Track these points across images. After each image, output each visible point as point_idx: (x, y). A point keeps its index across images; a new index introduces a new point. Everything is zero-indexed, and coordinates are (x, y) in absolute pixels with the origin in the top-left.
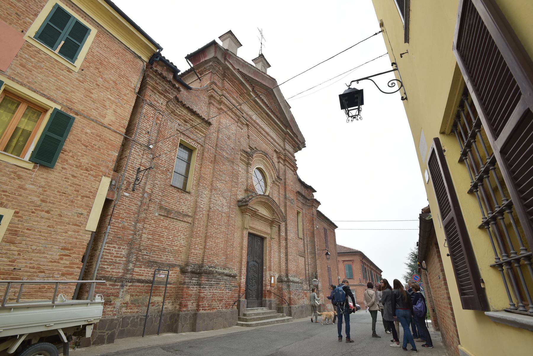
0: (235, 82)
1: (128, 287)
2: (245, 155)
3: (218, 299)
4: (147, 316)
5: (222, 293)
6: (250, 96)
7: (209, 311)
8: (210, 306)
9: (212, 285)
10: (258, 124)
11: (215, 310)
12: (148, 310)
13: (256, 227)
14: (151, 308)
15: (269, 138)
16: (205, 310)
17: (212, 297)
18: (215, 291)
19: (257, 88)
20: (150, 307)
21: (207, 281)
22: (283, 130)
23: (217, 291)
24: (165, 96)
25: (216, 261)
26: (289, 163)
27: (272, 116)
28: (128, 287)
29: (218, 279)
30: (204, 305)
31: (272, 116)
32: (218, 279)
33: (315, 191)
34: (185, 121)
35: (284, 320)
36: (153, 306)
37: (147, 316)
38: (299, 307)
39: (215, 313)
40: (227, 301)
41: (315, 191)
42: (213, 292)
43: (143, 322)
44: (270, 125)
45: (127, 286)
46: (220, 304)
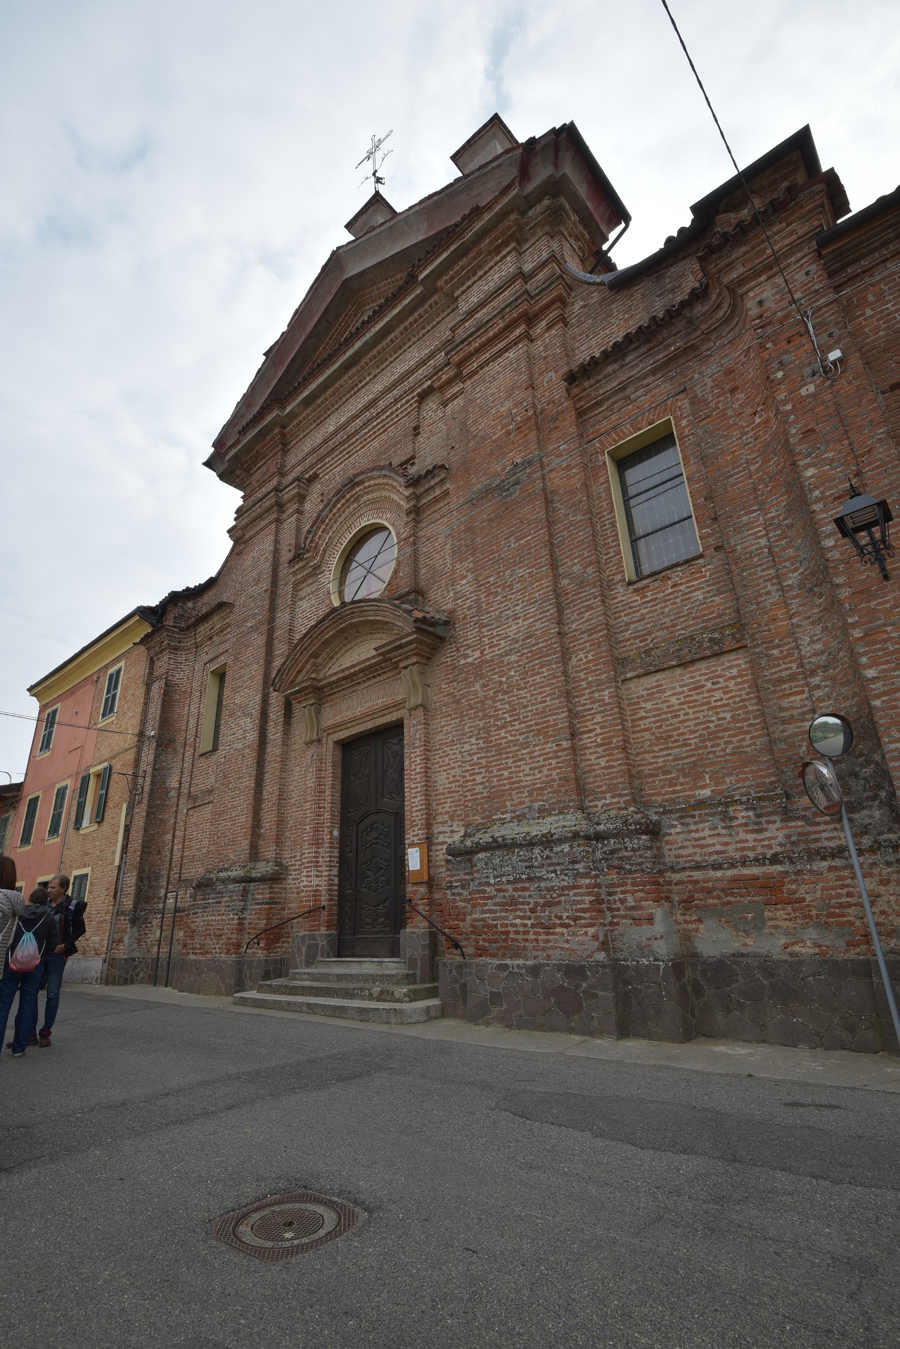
0: (258, 452)
2: (301, 564)
4: (158, 958)
6: (292, 415)
7: (201, 958)
8: (203, 946)
9: (205, 907)
13: (349, 715)
15: (382, 404)
16: (196, 954)
17: (206, 930)
21: (203, 899)
22: (420, 301)
23: (213, 918)
25: (232, 856)
26: (478, 351)
27: (358, 345)
29: (219, 893)
31: (358, 345)
35: (343, 1009)
38: (535, 971)
39: (206, 961)
40: (229, 939)
42: (208, 921)
44: (381, 362)
46: (218, 943)
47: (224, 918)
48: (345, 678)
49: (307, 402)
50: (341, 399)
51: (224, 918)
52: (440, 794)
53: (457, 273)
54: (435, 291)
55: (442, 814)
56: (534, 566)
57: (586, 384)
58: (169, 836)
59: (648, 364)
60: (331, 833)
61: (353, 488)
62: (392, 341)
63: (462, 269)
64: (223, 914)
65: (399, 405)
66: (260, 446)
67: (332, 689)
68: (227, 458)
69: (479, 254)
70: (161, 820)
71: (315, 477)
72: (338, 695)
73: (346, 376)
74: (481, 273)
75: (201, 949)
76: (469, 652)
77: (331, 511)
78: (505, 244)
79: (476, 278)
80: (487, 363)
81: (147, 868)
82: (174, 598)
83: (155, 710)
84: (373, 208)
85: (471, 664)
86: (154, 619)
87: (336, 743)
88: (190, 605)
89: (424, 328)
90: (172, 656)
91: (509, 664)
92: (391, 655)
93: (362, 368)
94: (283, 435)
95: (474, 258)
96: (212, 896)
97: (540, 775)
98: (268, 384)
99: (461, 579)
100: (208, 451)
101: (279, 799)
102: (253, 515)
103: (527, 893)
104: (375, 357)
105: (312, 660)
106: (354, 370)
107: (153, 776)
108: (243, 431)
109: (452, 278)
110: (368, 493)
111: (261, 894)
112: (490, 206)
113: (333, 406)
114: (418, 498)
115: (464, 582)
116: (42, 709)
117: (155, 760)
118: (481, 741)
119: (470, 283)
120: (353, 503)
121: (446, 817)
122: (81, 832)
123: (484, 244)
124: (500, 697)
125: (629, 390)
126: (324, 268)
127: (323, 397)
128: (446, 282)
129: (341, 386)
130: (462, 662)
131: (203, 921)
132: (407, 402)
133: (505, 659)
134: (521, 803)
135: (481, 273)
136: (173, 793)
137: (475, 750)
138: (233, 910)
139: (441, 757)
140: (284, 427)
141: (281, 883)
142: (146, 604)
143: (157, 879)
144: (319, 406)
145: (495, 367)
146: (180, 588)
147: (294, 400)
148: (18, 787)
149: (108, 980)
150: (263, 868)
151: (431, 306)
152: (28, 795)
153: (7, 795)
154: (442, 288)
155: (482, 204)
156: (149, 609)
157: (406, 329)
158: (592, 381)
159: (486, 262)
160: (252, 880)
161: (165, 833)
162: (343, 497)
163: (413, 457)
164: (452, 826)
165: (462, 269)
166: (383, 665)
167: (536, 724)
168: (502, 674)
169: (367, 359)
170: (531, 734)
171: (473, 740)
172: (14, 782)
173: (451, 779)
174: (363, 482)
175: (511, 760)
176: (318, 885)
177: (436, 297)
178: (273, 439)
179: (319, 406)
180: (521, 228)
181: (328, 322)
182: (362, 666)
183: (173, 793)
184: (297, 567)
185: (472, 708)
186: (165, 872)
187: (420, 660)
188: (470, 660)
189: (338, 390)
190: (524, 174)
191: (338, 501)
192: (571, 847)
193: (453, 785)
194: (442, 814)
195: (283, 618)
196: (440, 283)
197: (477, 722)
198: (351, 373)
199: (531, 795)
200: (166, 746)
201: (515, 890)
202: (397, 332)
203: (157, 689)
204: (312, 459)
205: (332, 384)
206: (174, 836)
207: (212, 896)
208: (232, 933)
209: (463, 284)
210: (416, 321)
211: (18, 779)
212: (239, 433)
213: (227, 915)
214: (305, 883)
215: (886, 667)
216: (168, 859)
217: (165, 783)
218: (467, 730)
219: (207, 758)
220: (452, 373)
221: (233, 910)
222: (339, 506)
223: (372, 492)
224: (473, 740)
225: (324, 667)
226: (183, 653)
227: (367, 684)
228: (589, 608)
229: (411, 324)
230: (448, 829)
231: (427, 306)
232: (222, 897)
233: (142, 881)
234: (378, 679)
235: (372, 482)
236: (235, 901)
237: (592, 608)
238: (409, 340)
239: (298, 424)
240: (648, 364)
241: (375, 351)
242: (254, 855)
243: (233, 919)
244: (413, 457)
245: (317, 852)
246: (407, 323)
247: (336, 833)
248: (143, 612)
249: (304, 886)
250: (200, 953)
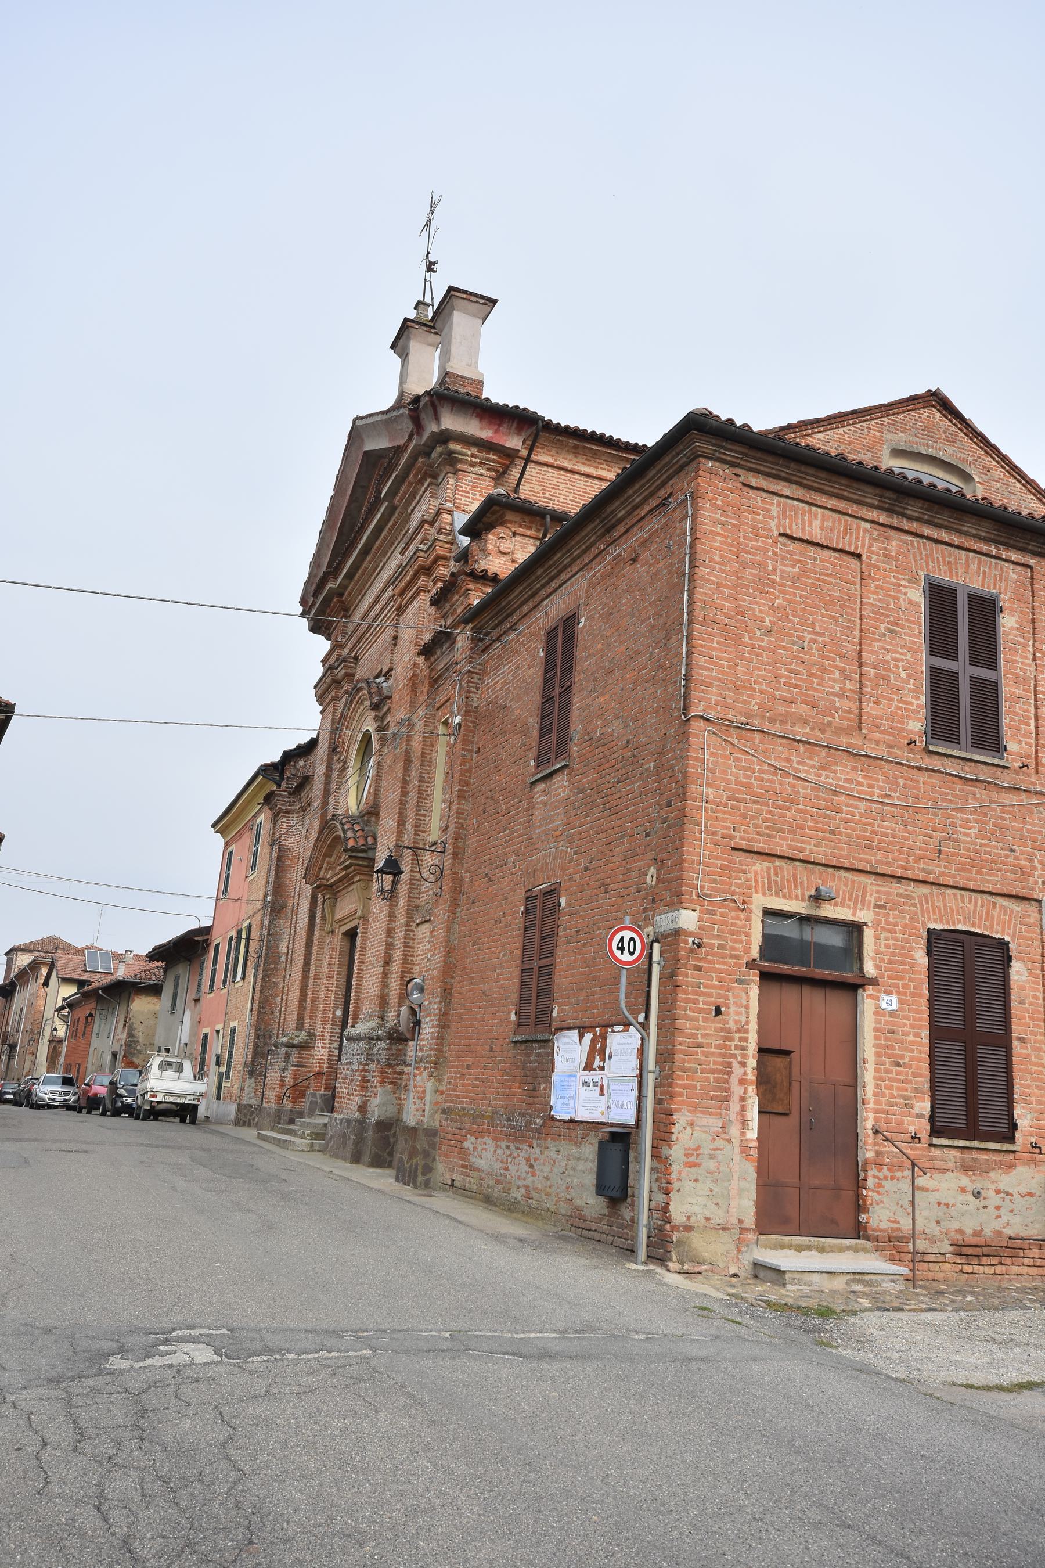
6: (343, 587)
15: (382, 602)
58: (279, 999)
60: (334, 1013)
69: (410, 484)
79: (415, 501)
81: (262, 1026)
82: (289, 756)
88: (301, 763)
90: (285, 820)
94: (343, 602)
98: (328, 546)
107: (268, 941)
108: (315, 595)
114: (382, 719)
116: (227, 844)
122: (237, 986)
126: (350, 435)
136: (283, 959)
140: (341, 595)
142: (268, 761)
148: (207, 930)
149: (237, 1123)
150: (303, 1035)
152: (216, 938)
153: (199, 938)
156: (274, 766)
159: (419, 490)
160: (293, 1046)
163: (391, 670)
172: (203, 925)
180: (431, 466)
181: (363, 487)
183: (283, 959)
186: (275, 1032)
187: (362, 877)
190: (418, 426)
191: (352, 701)
200: (279, 912)
211: (207, 922)
217: (278, 947)
242: (300, 1026)
244: (391, 670)
248: (266, 770)
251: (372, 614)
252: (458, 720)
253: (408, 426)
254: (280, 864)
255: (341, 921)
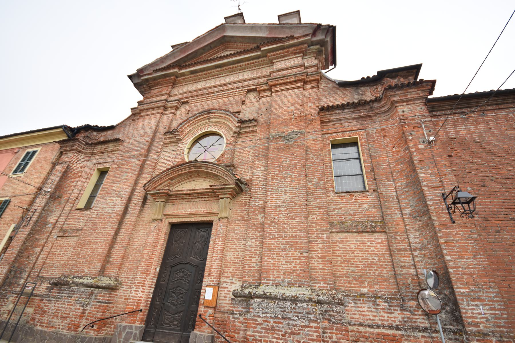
0: (159, 82)
1: (13, 298)
2: (171, 136)
3: (61, 317)
5: (70, 308)
6: (183, 75)
8: (49, 322)
9: (59, 298)
10: (203, 89)
11: (53, 330)
12: (20, 318)
13: (183, 212)
14: (23, 318)
15: (229, 87)
16: (42, 326)
17: (55, 312)
18: (60, 306)
19: (205, 56)
20: (22, 316)
21: (58, 293)
22: (258, 57)
23: (63, 306)
24: (73, 150)
25: (86, 270)
26: (281, 84)
28: (13, 298)
29: (72, 291)
30: (43, 321)
32: (72, 291)
33: (417, 68)
34: (103, 153)
36: (25, 316)
37: (17, 324)
39: (50, 332)
40: (72, 321)
41: (417, 68)
42: (59, 307)
43: (13, 329)
44: (232, 71)
45: (12, 297)
46: (62, 322)
47: (71, 307)
48: (186, 194)
49: (192, 72)
50: (208, 77)
51: (71, 307)
52: (228, 262)
53: (277, 54)
54: (266, 56)
55: (227, 272)
56: (297, 173)
57: (327, 113)
58: (39, 249)
59: (352, 116)
60: (156, 269)
61: (209, 113)
62: (240, 66)
63: (280, 54)
64: (72, 305)
65: (238, 90)
66: (161, 80)
67: (177, 197)
68: (142, 78)
69: (288, 52)
70: (36, 239)
71: (187, 102)
72: (178, 201)
73: (215, 70)
74: (286, 58)
75: (47, 324)
76: (257, 200)
77: (195, 119)
78: (299, 53)
80: (284, 90)
81: (17, 265)
82: (87, 128)
83: (55, 178)
84: (239, 17)
85: (257, 206)
86: (70, 134)
87: (170, 223)
88: (95, 133)
89: (255, 67)
90: (76, 154)
91: (279, 211)
92: (217, 191)
93: (223, 70)
94: (175, 80)
95: (286, 52)
96: (66, 292)
97: (290, 266)
98: (175, 58)
99: (258, 168)
100: (134, 71)
101: (127, 245)
102: (150, 106)
103: (281, 326)
104: (230, 68)
105: (169, 181)
106: (219, 69)
107: (41, 213)
109: (274, 55)
110: (215, 118)
111: (102, 296)
112: (298, 38)
113: (204, 78)
114: (241, 128)
115: (259, 169)
117: (45, 205)
118: (258, 242)
119: (281, 60)
120: (207, 119)
121: (230, 275)
123: (291, 49)
124: (273, 224)
125: (342, 122)
127: (201, 73)
128: (272, 55)
129: (211, 73)
130: (253, 204)
131: (55, 306)
132: (241, 90)
133: (278, 209)
134: (279, 277)
135: (286, 58)
136: (50, 225)
137: (254, 246)
138: (81, 303)
139: (232, 244)
140: (177, 77)
141: (116, 292)
143: (21, 273)
144: (197, 76)
145: (288, 93)
146: (92, 124)
147: (186, 69)
150: (105, 281)
151: (261, 61)
154: (269, 56)
155: (295, 36)
157: (248, 64)
158: (329, 113)
159: (289, 56)
161: (36, 247)
162: (202, 115)
163: (240, 112)
164: (232, 280)
165: (280, 54)
166: (210, 194)
167: (291, 242)
168: (275, 214)
169: (227, 67)
170: (288, 246)
171: (253, 241)
173: (236, 256)
174: (214, 113)
175: (276, 256)
176: (141, 297)
177: (265, 59)
178: (170, 79)
179: (197, 76)
180: (306, 51)
181: (211, 47)
182: (199, 191)
183: (50, 225)
184: (168, 136)
185: (255, 226)
188: (257, 204)
189: (209, 73)
190: (314, 34)
191: (200, 116)
192: (307, 305)
193: (237, 259)
194: (227, 272)
195: (152, 156)
196: (269, 54)
197: (257, 233)
198: (217, 69)
199: (284, 274)
200: (55, 199)
201: (274, 322)
202: (244, 63)
203: (60, 169)
204: (189, 95)
205: (207, 70)
206: (42, 250)
207: (66, 292)
208: (75, 318)
209: (278, 59)
210: (253, 63)
212: (154, 71)
213: (75, 305)
214: (133, 295)
215: (454, 257)
216: (33, 262)
217: (47, 218)
218: (250, 235)
219: (81, 211)
220: (266, 88)
221: (81, 303)
222: (199, 118)
223: (218, 118)
224: (253, 241)
225: (174, 185)
226: (83, 155)
227: (196, 200)
228: (320, 198)
229: (251, 63)
230: (230, 281)
231: (260, 60)
232: (74, 294)
233: (10, 273)
234: (204, 199)
235: (219, 115)
236: (83, 298)
237: (321, 198)
238: (248, 68)
239: (184, 79)
240: (352, 116)
241: (231, 66)
242: (102, 272)
243: (79, 309)
245: (145, 278)
246: (249, 62)
247: (158, 270)
248: (66, 128)
249: (132, 296)
250: (46, 327)
251: (216, 89)
252: (432, 138)
253: (311, 31)
254: (65, 175)
255: (168, 216)
